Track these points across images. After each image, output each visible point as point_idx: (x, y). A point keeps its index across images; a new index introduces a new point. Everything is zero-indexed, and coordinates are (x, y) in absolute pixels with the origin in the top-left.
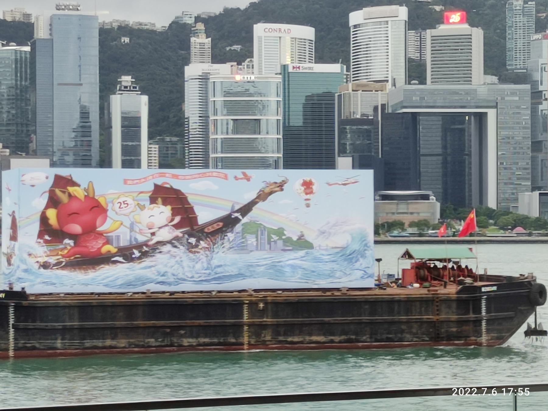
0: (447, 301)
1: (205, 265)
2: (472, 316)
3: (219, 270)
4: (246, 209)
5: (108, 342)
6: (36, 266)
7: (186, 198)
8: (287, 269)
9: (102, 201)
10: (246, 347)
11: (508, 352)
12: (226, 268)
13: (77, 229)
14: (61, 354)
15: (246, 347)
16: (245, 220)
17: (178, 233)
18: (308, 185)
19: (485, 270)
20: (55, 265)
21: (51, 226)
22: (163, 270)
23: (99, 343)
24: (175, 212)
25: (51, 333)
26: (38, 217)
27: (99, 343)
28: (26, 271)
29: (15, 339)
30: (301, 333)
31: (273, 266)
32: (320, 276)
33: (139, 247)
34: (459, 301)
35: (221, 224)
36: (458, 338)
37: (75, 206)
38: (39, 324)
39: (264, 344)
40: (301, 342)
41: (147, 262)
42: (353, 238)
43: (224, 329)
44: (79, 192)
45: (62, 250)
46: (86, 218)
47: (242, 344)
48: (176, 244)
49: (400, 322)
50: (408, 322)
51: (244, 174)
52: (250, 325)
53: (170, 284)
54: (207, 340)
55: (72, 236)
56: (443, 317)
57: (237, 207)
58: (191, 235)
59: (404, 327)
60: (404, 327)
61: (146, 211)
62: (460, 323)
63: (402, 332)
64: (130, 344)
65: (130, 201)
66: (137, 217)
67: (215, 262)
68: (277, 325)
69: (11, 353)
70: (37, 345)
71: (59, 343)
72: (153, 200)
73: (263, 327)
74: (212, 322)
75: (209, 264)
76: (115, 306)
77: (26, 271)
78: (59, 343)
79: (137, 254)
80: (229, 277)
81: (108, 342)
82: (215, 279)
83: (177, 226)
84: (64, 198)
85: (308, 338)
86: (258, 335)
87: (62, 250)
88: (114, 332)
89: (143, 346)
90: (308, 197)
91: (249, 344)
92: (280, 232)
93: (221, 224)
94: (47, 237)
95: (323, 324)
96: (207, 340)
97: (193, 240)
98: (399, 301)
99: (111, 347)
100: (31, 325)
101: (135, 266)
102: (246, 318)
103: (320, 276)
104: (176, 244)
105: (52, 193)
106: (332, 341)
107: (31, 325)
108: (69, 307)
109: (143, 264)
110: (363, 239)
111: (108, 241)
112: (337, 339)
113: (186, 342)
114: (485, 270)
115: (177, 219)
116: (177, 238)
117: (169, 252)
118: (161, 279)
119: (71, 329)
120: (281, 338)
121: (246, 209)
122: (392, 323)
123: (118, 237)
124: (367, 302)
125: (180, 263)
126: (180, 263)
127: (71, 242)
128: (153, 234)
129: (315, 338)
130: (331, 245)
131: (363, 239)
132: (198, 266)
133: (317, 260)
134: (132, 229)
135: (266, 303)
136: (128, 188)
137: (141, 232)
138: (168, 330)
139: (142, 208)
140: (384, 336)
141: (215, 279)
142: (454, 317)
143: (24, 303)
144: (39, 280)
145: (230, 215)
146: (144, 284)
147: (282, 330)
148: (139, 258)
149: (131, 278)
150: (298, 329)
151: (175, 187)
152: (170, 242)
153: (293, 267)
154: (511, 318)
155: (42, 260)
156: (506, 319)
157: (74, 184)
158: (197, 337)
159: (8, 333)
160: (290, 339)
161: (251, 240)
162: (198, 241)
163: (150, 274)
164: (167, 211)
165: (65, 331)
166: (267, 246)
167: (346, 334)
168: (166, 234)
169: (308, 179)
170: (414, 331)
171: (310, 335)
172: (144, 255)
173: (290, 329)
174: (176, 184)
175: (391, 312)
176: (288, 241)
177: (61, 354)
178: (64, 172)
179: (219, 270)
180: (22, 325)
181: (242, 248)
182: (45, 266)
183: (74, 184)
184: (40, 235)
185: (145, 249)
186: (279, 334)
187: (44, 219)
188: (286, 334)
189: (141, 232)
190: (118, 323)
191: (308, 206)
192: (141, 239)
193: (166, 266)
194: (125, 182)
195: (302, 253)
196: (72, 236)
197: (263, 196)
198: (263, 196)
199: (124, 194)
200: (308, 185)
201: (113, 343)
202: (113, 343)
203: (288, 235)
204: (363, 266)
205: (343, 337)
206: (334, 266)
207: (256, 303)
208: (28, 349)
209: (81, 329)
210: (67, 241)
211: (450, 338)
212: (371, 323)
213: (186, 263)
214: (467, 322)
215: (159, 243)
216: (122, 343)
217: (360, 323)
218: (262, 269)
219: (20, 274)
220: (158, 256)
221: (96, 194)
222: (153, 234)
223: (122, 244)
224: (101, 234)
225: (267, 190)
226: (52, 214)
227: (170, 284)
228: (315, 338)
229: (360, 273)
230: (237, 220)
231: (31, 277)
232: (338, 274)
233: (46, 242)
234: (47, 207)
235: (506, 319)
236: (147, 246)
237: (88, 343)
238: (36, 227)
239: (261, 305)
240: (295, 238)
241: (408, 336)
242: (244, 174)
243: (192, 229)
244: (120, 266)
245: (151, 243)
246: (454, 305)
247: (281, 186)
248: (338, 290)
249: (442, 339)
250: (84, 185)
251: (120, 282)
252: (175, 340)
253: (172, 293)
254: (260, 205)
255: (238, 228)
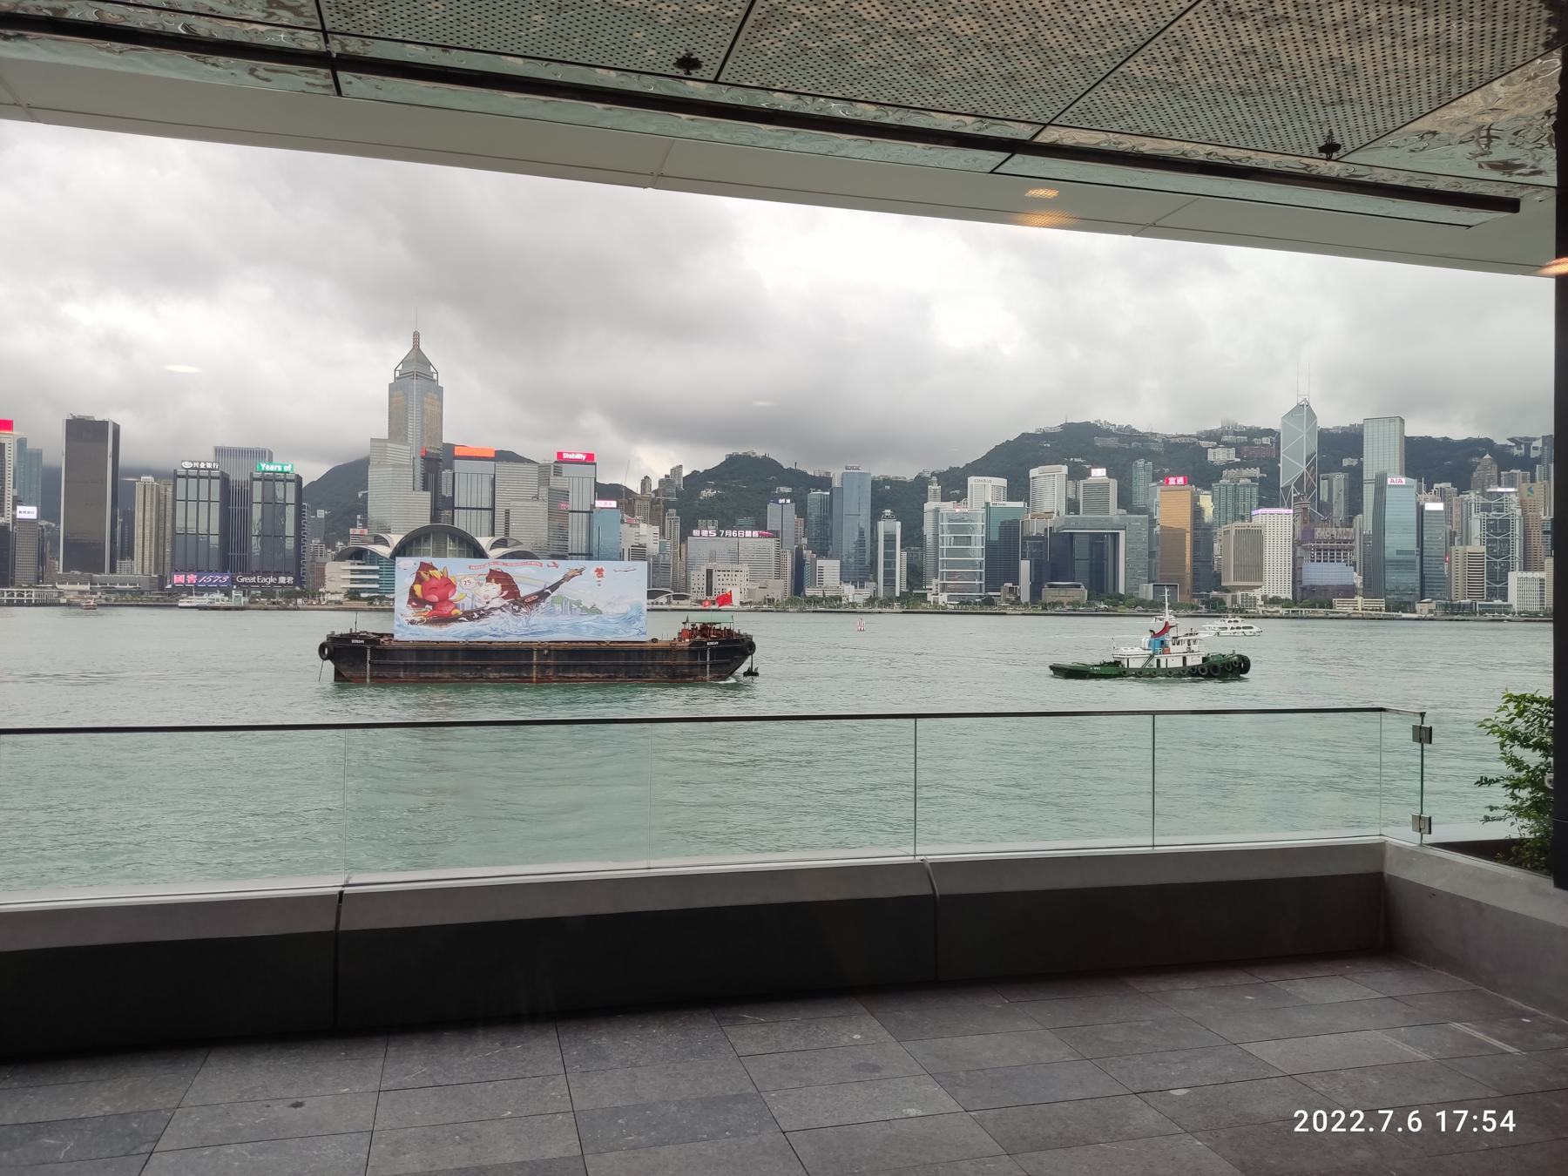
0: (682, 651)
1: (525, 624)
2: (699, 661)
3: (534, 627)
4: (554, 587)
5: (437, 675)
6: (406, 623)
7: (512, 579)
8: (584, 628)
9: (453, 580)
10: (534, 680)
11: (736, 687)
12: (541, 626)
13: (435, 598)
14: (402, 682)
15: (534, 680)
16: (553, 594)
17: (506, 602)
18: (599, 572)
19: (739, 630)
20: (420, 622)
21: (416, 596)
22: (495, 626)
23: (431, 675)
24: (503, 588)
25: (397, 666)
26: (408, 590)
27: (431, 675)
28: (399, 626)
29: (371, 671)
30: (575, 671)
31: (573, 625)
32: (608, 633)
33: (478, 611)
34: (690, 651)
35: (537, 597)
36: (689, 677)
37: (434, 583)
38: (389, 661)
39: (548, 679)
40: (575, 678)
41: (483, 621)
42: (632, 609)
43: (518, 667)
44: (437, 574)
45: (424, 612)
46: (442, 591)
47: (532, 678)
48: (504, 609)
49: (647, 665)
50: (652, 665)
51: (554, 563)
52: (538, 665)
53: (500, 636)
54: (507, 674)
55: (430, 603)
56: (678, 662)
57: (548, 586)
58: (514, 604)
59: (650, 668)
60: (650, 668)
61: (483, 587)
62: (691, 666)
63: (649, 671)
64: (452, 676)
65: (472, 580)
66: (477, 592)
67: (532, 622)
68: (558, 665)
69: (368, 680)
70: (386, 675)
71: (402, 674)
72: (488, 580)
73: (547, 666)
74: (511, 662)
75: (527, 623)
76: (441, 650)
77: (399, 626)
78: (402, 674)
79: (476, 615)
80: (542, 633)
81: (437, 675)
82: (531, 634)
83: (504, 598)
84: (427, 578)
85: (579, 675)
86: (544, 672)
87: (424, 612)
88: (441, 668)
89: (461, 678)
90: (600, 579)
91: (537, 678)
92: (579, 603)
93: (537, 597)
94: (414, 604)
95: (591, 665)
96: (507, 674)
97: (516, 607)
98: (647, 651)
99: (439, 678)
100: (382, 661)
101: (475, 623)
102: (535, 659)
103: (608, 633)
104: (504, 609)
105: (418, 574)
106: (597, 677)
107: (382, 661)
108: (410, 650)
109: (481, 623)
110: (639, 609)
111: (456, 607)
112: (601, 675)
113: (491, 675)
114: (739, 630)
115: (505, 593)
116: (505, 606)
117: (499, 615)
118: (493, 633)
119: (411, 665)
120: (560, 674)
121: (554, 587)
122: (641, 665)
123: (463, 605)
124: (623, 651)
125: (507, 623)
126: (507, 623)
127: (431, 607)
128: (488, 603)
129: (584, 675)
130: (615, 611)
131: (639, 609)
132: (520, 625)
133: (604, 622)
134: (473, 599)
135: (550, 651)
136: (470, 571)
137: (479, 601)
138: (479, 667)
139: (481, 585)
140: (636, 674)
141: (531, 634)
142: (686, 662)
143: (378, 647)
144: (408, 632)
145: (543, 591)
146: (481, 636)
147: (561, 669)
148: (478, 618)
149: (472, 632)
150: (574, 668)
151: (505, 571)
152: (500, 608)
153: (587, 626)
154: (728, 664)
155: (410, 619)
156: (728, 664)
157: (434, 568)
158: (500, 672)
159: (366, 667)
160: (566, 675)
161: (558, 608)
162: (520, 608)
163: (483, 629)
164: (498, 587)
165: (406, 666)
166: (569, 612)
167: (608, 672)
168: (497, 603)
169: (600, 568)
170: (657, 671)
171: (581, 672)
172: (481, 616)
173: (567, 668)
174: (505, 570)
175: (641, 658)
176: (584, 609)
177: (402, 682)
178: (427, 560)
179: (534, 627)
180: (376, 661)
181: (551, 613)
182: (412, 622)
183: (434, 568)
184: (409, 602)
185: (482, 612)
186: (559, 672)
187: (412, 591)
188: (564, 672)
189: (479, 601)
190: (444, 662)
191: (599, 585)
192: (480, 606)
193: (497, 624)
194: (470, 567)
195: (594, 617)
196: (430, 603)
197: (567, 578)
198: (567, 578)
199: (469, 575)
200: (599, 572)
201: (440, 675)
202: (440, 675)
203: (584, 605)
204: (639, 626)
205: (605, 675)
206: (620, 627)
207: (543, 650)
208: (381, 677)
209: (418, 665)
210: (427, 606)
211: (683, 676)
212: (625, 665)
213: (511, 622)
214: (696, 665)
215: (492, 608)
216: (447, 675)
217: (618, 665)
218: (565, 627)
219: (396, 628)
220: (492, 617)
221: (449, 574)
222: (488, 603)
223: (466, 609)
224: (451, 602)
225: (570, 574)
226: (418, 588)
227: (500, 636)
228: (584, 675)
229: (636, 632)
230: (548, 594)
231: (403, 630)
232: (621, 631)
233: (413, 606)
234: (414, 584)
235: (724, 664)
236: (483, 610)
237: (422, 675)
238: (407, 596)
239: (546, 652)
240: (589, 607)
241: (653, 674)
242: (554, 563)
243: (516, 600)
244: (464, 623)
245: (486, 609)
246: (687, 654)
247: (580, 572)
248: (604, 642)
249: (677, 677)
250: (440, 569)
251: (464, 634)
252: (484, 674)
253: (491, 642)
254: (565, 584)
255: (549, 599)
